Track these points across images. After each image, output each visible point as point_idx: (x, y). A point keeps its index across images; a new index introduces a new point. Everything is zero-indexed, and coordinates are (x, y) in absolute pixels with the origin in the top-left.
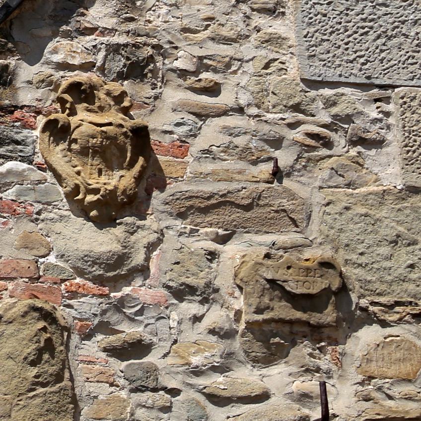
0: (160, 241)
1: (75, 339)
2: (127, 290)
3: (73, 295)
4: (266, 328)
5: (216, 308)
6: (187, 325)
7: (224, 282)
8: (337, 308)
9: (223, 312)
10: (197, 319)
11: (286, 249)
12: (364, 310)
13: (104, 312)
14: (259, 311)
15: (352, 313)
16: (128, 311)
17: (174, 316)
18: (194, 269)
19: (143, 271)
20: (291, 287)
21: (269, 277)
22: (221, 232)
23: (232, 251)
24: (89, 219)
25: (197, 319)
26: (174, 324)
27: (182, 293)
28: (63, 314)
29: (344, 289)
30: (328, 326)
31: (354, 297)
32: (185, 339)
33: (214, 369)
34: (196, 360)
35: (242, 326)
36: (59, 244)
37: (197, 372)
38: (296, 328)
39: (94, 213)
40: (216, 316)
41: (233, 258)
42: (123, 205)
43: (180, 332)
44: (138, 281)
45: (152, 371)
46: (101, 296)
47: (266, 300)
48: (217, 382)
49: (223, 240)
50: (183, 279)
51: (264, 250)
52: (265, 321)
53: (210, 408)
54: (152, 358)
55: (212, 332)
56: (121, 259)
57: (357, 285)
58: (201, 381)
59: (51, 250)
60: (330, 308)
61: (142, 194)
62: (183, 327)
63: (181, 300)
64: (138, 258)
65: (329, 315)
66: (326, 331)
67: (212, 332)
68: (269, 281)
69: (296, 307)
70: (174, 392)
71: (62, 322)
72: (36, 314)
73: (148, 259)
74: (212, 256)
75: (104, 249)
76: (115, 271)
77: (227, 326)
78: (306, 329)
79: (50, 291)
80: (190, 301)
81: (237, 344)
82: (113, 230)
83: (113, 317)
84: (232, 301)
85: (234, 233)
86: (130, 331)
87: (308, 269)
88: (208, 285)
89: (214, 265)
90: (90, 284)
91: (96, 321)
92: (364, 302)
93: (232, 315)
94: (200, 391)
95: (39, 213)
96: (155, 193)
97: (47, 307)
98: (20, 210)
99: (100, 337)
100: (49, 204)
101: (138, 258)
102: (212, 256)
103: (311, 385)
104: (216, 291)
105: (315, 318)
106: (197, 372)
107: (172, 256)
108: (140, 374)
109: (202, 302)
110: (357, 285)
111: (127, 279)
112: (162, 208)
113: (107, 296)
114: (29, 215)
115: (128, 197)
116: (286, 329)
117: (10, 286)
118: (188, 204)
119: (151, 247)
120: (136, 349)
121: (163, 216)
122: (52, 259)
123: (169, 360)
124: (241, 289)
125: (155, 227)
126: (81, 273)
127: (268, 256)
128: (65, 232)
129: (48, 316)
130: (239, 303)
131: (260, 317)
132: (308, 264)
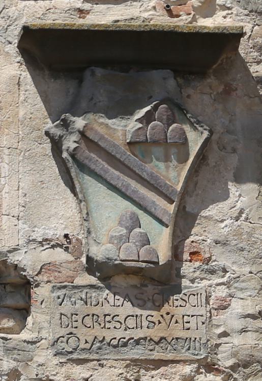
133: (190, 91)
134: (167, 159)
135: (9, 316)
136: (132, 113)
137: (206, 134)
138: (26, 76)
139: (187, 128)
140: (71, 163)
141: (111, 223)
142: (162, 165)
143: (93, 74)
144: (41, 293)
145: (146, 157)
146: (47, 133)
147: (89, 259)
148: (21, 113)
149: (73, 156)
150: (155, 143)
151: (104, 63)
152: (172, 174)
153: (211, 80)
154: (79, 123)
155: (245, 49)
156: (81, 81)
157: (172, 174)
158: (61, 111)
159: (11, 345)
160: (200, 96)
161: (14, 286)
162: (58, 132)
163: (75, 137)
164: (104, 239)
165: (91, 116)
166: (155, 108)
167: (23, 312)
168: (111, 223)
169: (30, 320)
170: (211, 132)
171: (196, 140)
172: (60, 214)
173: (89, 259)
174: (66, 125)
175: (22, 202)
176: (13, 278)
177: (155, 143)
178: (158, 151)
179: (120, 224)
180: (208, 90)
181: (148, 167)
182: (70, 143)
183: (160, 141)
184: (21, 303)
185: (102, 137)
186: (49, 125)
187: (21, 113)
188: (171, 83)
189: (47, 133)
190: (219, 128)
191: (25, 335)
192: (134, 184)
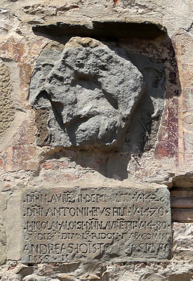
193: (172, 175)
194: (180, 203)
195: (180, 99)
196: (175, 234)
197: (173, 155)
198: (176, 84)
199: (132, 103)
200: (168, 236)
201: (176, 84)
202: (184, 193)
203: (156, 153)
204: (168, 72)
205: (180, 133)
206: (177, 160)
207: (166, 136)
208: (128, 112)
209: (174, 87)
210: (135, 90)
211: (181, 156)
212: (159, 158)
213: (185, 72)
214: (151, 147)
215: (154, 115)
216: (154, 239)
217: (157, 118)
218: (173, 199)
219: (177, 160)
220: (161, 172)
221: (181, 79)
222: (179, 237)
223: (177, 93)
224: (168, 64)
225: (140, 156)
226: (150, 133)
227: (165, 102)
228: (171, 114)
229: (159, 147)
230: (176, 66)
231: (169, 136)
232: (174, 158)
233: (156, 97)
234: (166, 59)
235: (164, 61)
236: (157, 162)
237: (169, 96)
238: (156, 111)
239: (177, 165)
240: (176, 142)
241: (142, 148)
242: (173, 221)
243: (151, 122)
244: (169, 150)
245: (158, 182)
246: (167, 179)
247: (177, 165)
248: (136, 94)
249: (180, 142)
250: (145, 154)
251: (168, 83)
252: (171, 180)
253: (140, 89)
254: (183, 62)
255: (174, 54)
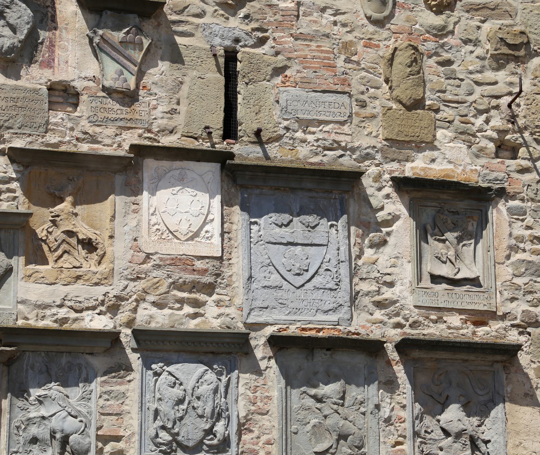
0: (459, 21)
1: (425, 58)
2: (445, 40)
3: (425, 41)
4: (498, 57)
5: (479, 48)
6: (468, 54)
7: (483, 38)
8: (525, 50)
9: (482, 50)
10: (472, 52)
11: (507, 26)
12: (536, 51)
13: (437, 48)
14: (496, 50)
15: (531, 52)
16: (446, 48)
17: (463, 50)
18: (472, 33)
19: (452, 32)
20: (508, 41)
21: (500, 37)
22: (482, 18)
23: (486, 26)
24: (432, 11)
25: (472, 52)
26: (463, 54)
27: (466, 42)
28: (421, 48)
29: (528, 43)
30: (522, 57)
31: (532, 46)
32: (467, 60)
33: (477, 72)
34: (471, 68)
35: (489, 56)
36: (420, 20)
37: (471, 73)
38: (509, 57)
39: (434, 9)
40: (479, 51)
41: (487, 29)
42: (446, 6)
43: (465, 57)
44: (450, 37)
45: (454, 71)
46: (436, 42)
47: (499, 46)
48: (478, 77)
49: (483, 22)
50: (467, 37)
51: (499, 26)
52: (498, 54)
53: (475, 87)
54: (454, 67)
55: (477, 57)
56: (444, 27)
57: (533, 41)
58: (472, 76)
59: (417, 23)
60: (523, 50)
61: (453, 2)
62: (466, 55)
63: (466, 45)
64: (451, 28)
65: (522, 53)
66: (521, 59)
67: (477, 57)
68: (500, 38)
69: (510, 49)
70: (462, 80)
71: (420, 51)
72: (411, 48)
73: (454, 28)
74: (479, 28)
75: (438, 23)
76: (441, 32)
77: (483, 55)
78: (513, 58)
79: (416, 39)
80: (470, 45)
81: (486, 63)
82: (441, 16)
83: (440, 50)
84: (485, 45)
85: (487, 19)
86: (446, 56)
87: (515, 34)
88: (477, 39)
89: (479, 31)
90: (431, 37)
91: (433, 52)
92: (536, 48)
93: (485, 51)
94: (472, 80)
95: (413, 8)
96: (458, 2)
97: (415, 45)
98: (406, 6)
99: (434, 58)
100: (417, 5)
101: (451, 28)
102: (479, 28)
103: (516, 79)
104: (480, 41)
105: (517, 53)
106: (471, 73)
107: (464, 27)
108: (449, 72)
109: (474, 46)
110: (533, 41)
111: (446, 35)
112: (461, 8)
113: (438, 42)
114: (409, 8)
115: (448, 3)
116: (506, 57)
117: (401, 36)
118: (470, 7)
119: (456, 23)
120: (448, 63)
121: (461, 11)
122: (417, 26)
123: (460, 68)
124: (489, 41)
125: (457, 15)
126: (428, 32)
127: (500, 29)
128: (423, 16)
129: (415, 49)
130: (488, 47)
131: (496, 52)
132: (515, 32)
133: (144, 24)
134: (135, 50)
135: (70, 106)
136: (121, 30)
137: (150, 41)
138: (79, 11)
139: (143, 38)
140: (97, 48)
141: (112, 73)
142: (133, 52)
143: (106, 13)
144: (84, 98)
145: (126, 48)
146: (87, 35)
147: (103, 86)
148: (77, 26)
149: (97, 45)
150: (130, 42)
151: (111, 9)
152: (137, 55)
153: (152, 20)
154: (100, 32)
155: (166, 9)
156: (101, 16)
157: (137, 55)
158: (93, 27)
159: (71, 117)
160: (148, 26)
161: (72, 94)
162: (92, 35)
163: (98, 38)
164: (109, 78)
165: (105, 30)
166: (131, 29)
167: (76, 105)
168: (112, 73)
169: (78, 108)
170: (152, 40)
171: (146, 43)
172: (92, 67)
173: (103, 86)
174: (95, 32)
175: (76, 61)
176: (72, 91)
177: (130, 42)
178: (131, 46)
179: (116, 73)
180: (151, 24)
181: (127, 52)
182: (97, 40)
183: (132, 42)
184: (75, 102)
185: (109, 39)
186: (88, 32)
187: (77, 26)
188: (137, 20)
189: (87, 35)
190: (155, 39)
191: (76, 114)
192: (121, 58)
193: (50, 80)
194: (54, 99)
195: (57, 32)
196: (50, 118)
197: (51, 67)
198: (55, 22)
199: (25, 32)
200: (46, 119)
201: (55, 22)
202: (57, 93)
203: (40, 65)
204: (50, 15)
205: (56, 54)
206: (53, 71)
207: (47, 55)
208: (23, 37)
209: (54, 25)
210: (28, 23)
211: (56, 69)
212: (42, 69)
213: (61, 16)
214: (37, 61)
215: (39, 41)
216: (36, 120)
217: (42, 43)
218: (50, 95)
219: (53, 71)
220: (43, 78)
221: (58, 20)
222: (53, 120)
223: (56, 29)
224: (50, 9)
225: (29, 66)
226: (36, 52)
227: (47, 34)
228: (51, 42)
229: (42, 62)
230: (55, 11)
231: (49, 56)
232: (52, 70)
233: (41, 30)
234: (49, 6)
235: (48, 7)
236: (41, 71)
237: (50, 30)
238: (41, 39)
239: (53, 74)
240: (54, 60)
241: (31, 61)
242: (49, 110)
243: (38, 46)
244: (49, 64)
245: (40, 84)
246: (47, 83)
247: (53, 74)
248: (29, 26)
249: (56, 60)
250: (32, 65)
251: (50, 22)
252: (49, 83)
253: (31, 24)
254: (60, 9)
255: (54, 3)
